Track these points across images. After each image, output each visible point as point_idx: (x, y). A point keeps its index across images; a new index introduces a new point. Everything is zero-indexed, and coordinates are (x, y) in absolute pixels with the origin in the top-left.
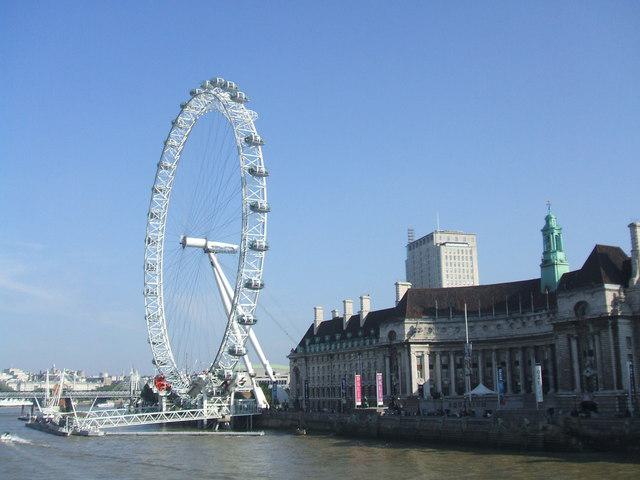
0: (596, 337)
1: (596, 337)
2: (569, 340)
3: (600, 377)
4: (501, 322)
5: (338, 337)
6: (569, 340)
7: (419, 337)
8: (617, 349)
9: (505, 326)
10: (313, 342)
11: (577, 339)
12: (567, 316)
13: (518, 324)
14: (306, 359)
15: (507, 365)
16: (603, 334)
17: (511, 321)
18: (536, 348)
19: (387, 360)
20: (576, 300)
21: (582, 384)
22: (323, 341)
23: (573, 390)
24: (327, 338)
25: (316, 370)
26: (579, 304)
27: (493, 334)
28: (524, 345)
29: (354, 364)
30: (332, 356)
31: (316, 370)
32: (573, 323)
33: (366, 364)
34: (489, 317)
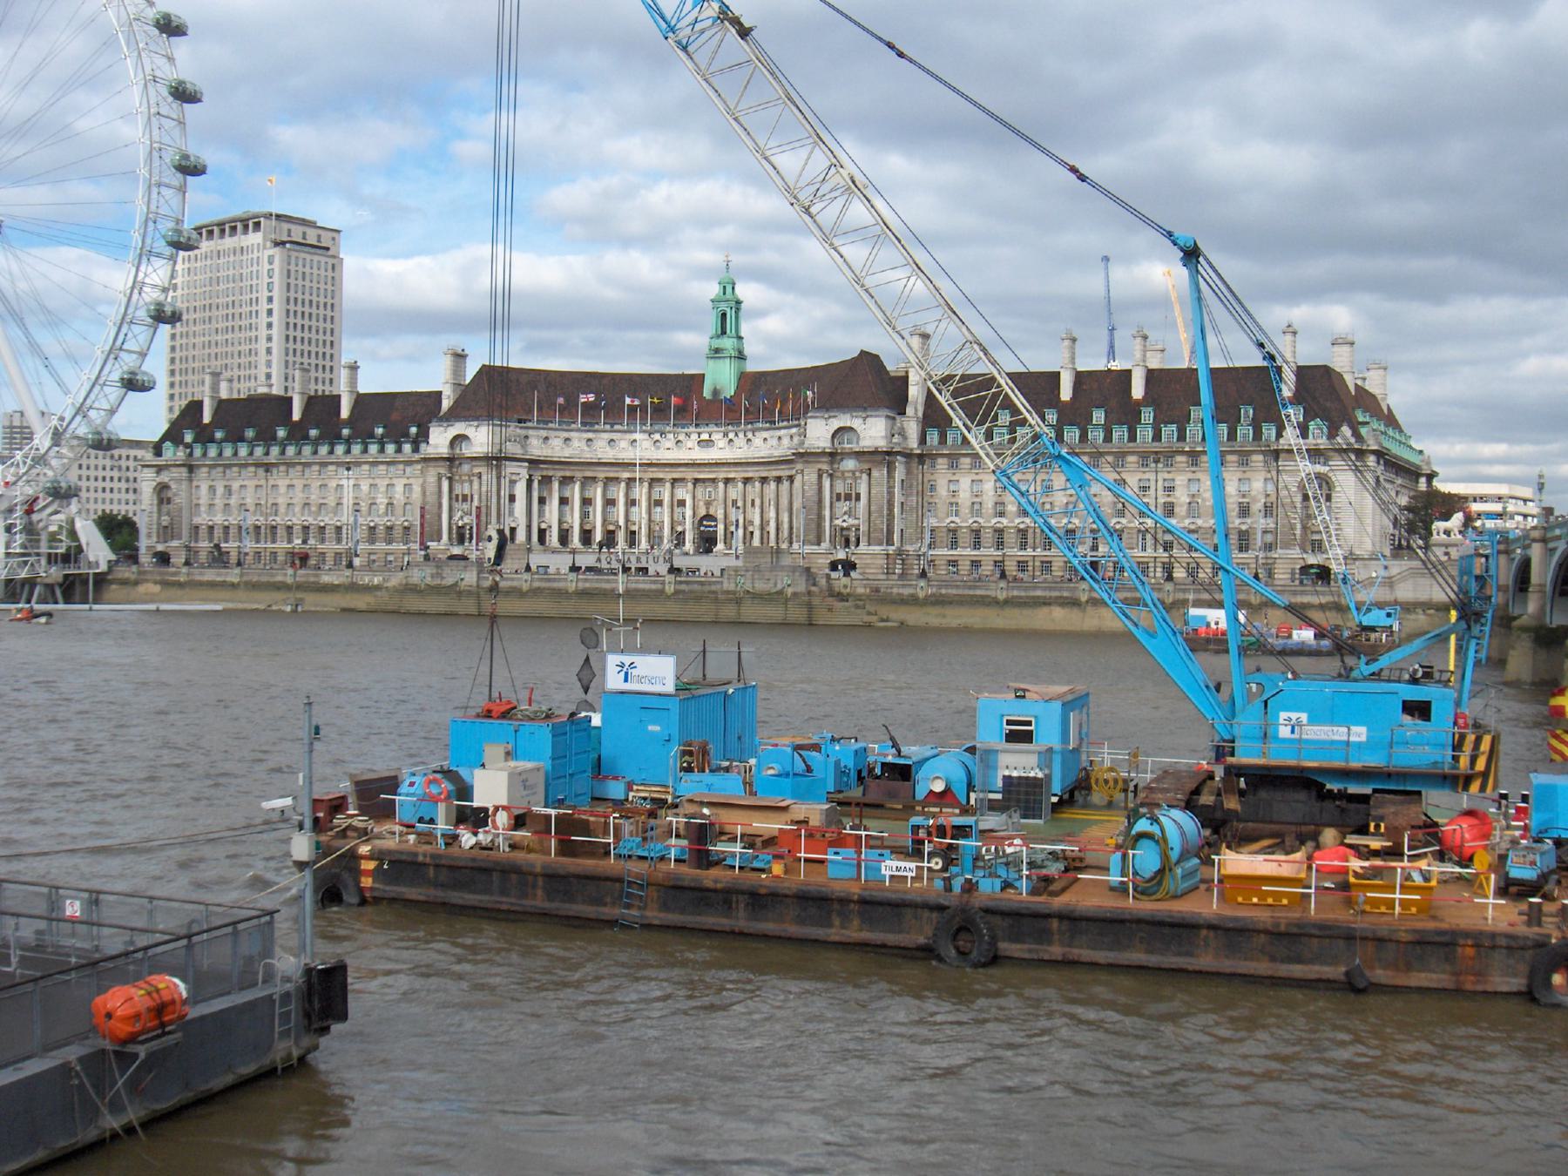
1: (865, 476)
2: (820, 477)
4: (637, 436)
5: (281, 433)
6: (820, 477)
7: (513, 449)
8: (891, 494)
9: (647, 444)
10: (204, 436)
12: (822, 444)
13: (669, 441)
14: (191, 469)
16: (875, 473)
17: (657, 436)
18: (696, 481)
19: (445, 484)
20: (836, 424)
22: (236, 438)
23: (819, 544)
24: (250, 433)
26: (840, 430)
28: (676, 476)
29: (333, 484)
30: (268, 468)
31: (220, 490)
33: (365, 487)
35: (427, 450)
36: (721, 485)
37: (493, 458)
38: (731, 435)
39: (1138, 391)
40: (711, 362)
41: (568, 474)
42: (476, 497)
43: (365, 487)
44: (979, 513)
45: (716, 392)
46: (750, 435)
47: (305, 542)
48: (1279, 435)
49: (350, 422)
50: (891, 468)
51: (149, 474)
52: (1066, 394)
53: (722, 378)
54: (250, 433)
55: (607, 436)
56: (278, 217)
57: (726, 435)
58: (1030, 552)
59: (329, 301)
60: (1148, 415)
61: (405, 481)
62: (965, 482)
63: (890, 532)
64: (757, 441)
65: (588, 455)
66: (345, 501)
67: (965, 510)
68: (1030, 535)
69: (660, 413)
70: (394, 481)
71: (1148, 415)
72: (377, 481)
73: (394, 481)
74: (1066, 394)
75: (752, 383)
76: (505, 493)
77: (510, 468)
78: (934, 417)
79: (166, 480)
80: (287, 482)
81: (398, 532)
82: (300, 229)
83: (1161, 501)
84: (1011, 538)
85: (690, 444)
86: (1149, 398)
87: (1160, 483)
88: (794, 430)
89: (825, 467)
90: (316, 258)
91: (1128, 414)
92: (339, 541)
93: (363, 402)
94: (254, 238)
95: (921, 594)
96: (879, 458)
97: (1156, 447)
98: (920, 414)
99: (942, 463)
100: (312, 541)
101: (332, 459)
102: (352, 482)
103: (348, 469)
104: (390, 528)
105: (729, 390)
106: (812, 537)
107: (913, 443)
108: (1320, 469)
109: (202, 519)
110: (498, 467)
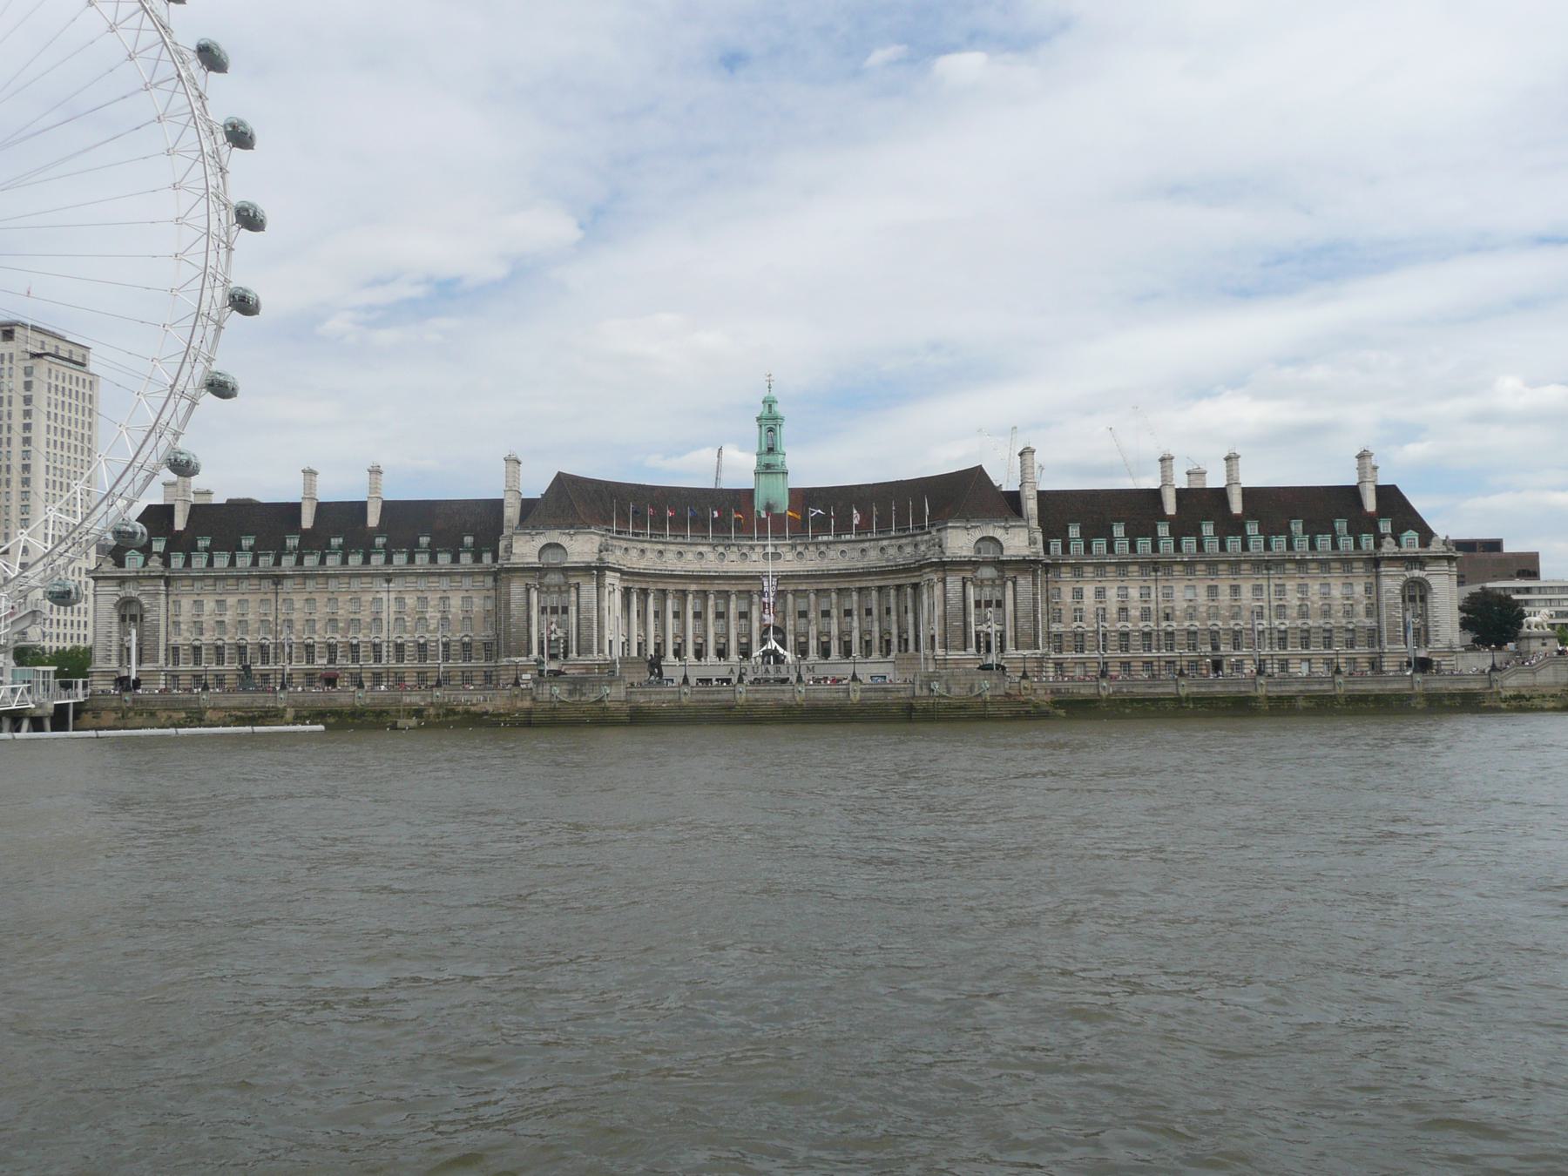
0: (1010, 584)
1: (1010, 584)
3: (1009, 634)
4: (701, 549)
8: (1035, 600)
10: (182, 543)
11: (975, 586)
13: (733, 554)
14: (168, 581)
15: (711, 616)
16: (1021, 581)
17: (721, 549)
19: (534, 595)
20: (978, 534)
21: (978, 642)
25: (209, 605)
26: (983, 539)
27: (690, 567)
30: (278, 580)
31: (209, 605)
33: (411, 600)
34: (680, 540)
36: (812, 596)
37: (596, 568)
38: (799, 549)
39: (1237, 507)
40: (762, 477)
42: (573, 609)
43: (411, 600)
44: (1104, 619)
45: (769, 508)
46: (823, 548)
47: (331, 661)
48: (1378, 545)
49: (380, 530)
51: (111, 588)
52: (1170, 508)
53: (776, 494)
54: (247, 542)
56: (34, 328)
57: (793, 547)
58: (1154, 653)
59: (87, 419)
60: (1252, 528)
61: (464, 594)
62: (1089, 590)
63: (1036, 636)
64: (833, 553)
66: (384, 616)
67: (1090, 615)
69: (721, 527)
70: (449, 594)
71: (1252, 528)
72: (429, 595)
73: (449, 594)
74: (1170, 508)
75: (804, 498)
79: (134, 594)
80: (306, 596)
81: (455, 648)
82: (54, 342)
84: (1136, 640)
85: (754, 557)
87: (1272, 588)
88: (885, 543)
89: (969, 575)
90: (75, 374)
91: (1230, 526)
92: (378, 659)
93: (391, 509)
95: (1104, 693)
96: (1025, 566)
97: (1267, 556)
99: (1066, 574)
100: (342, 662)
101: (369, 569)
102: (393, 596)
103: (389, 581)
104: (446, 645)
105: (783, 505)
106: (959, 642)
108: (1417, 573)
109: (185, 638)
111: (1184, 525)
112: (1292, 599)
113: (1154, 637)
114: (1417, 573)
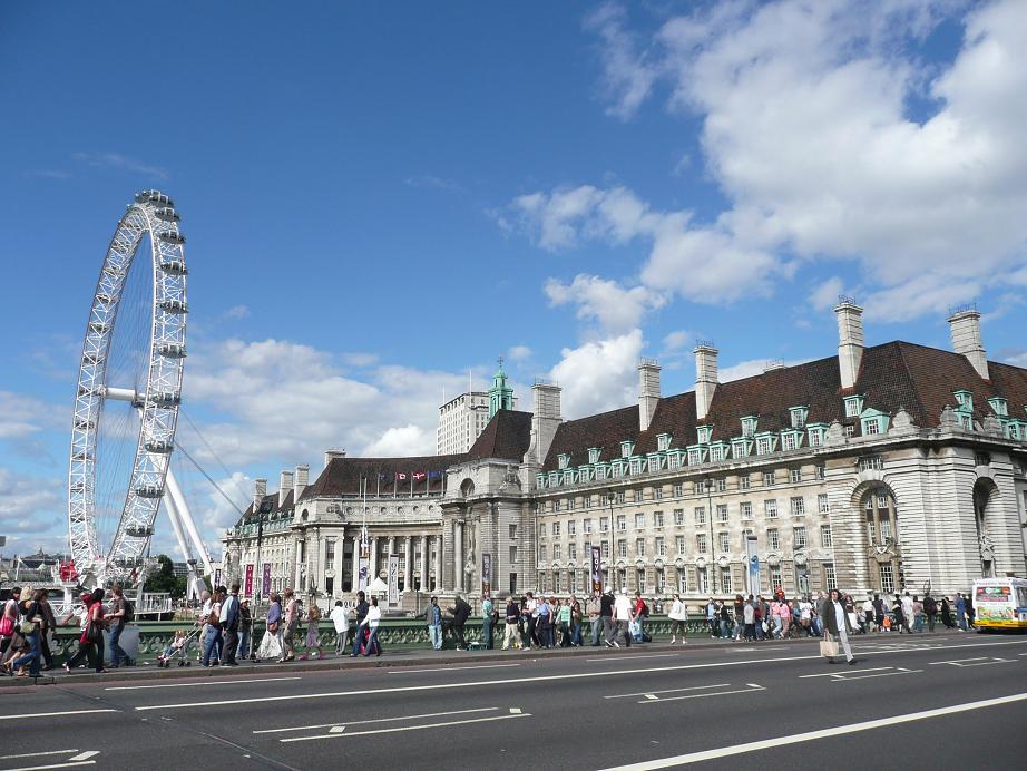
4: (432, 502)
6: (453, 526)
7: (334, 518)
16: (483, 520)
19: (299, 545)
20: (462, 476)
32: (458, 505)
35: (294, 522)
39: (702, 411)
41: (383, 535)
50: (494, 511)
52: (644, 425)
55: (411, 503)
60: (704, 435)
65: (398, 518)
68: (610, 576)
74: (644, 425)
76: (323, 551)
77: (325, 532)
78: (550, 464)
83: (717, 531)
86: (712, 419)
94: (461, 407)
98: (541, 460)
107: (526, 490)
108: (871, 474)
110: (318, 531)
111: (645, 445)
112: (735, 523)
113: (610, 571)
114: (871, 474)
